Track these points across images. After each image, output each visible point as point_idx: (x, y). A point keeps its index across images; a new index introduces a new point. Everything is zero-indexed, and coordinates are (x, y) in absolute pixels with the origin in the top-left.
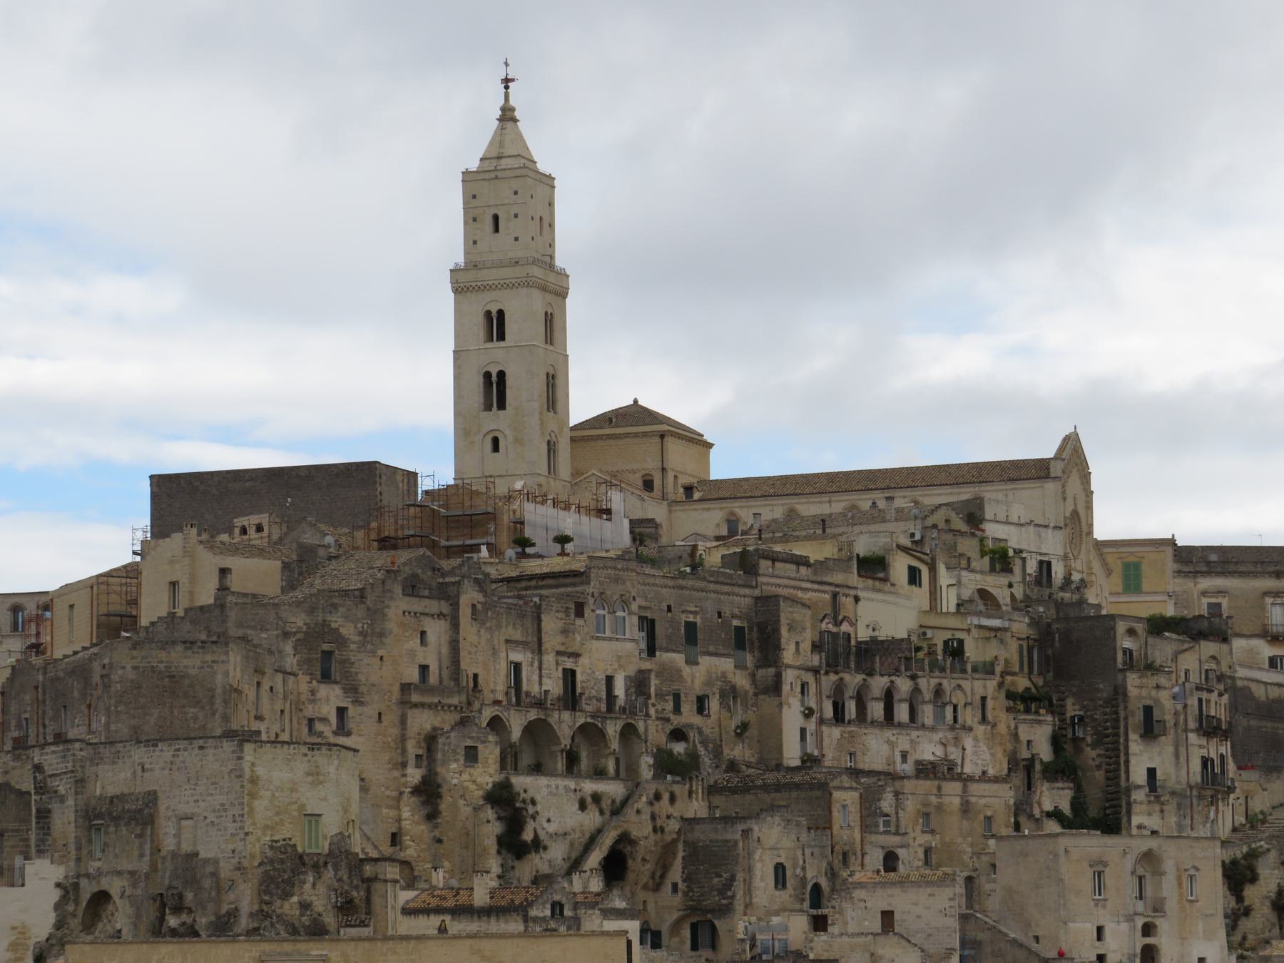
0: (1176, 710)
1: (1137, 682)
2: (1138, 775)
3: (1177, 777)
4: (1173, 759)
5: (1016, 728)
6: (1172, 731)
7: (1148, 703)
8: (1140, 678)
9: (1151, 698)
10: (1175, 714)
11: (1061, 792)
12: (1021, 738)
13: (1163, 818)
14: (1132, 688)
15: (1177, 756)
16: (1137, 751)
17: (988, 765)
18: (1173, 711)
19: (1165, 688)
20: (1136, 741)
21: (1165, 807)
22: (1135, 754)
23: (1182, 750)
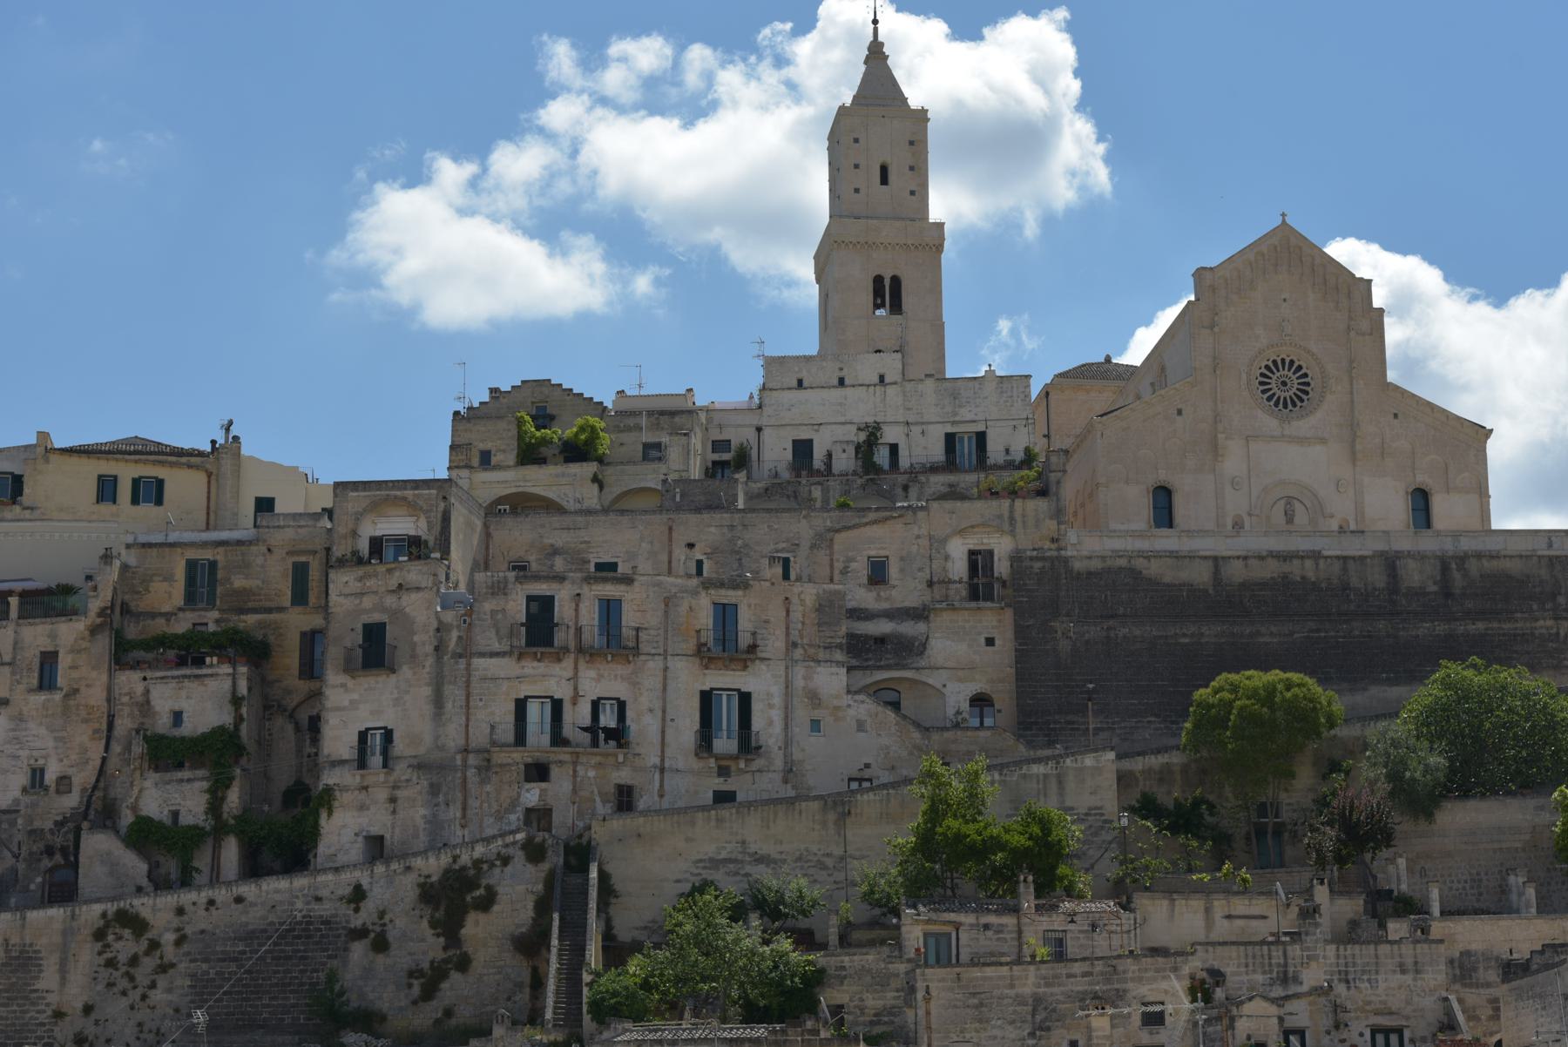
0: (440, 622)
1: (355, 586)
2: (338, 739)
3: (437, 738)
4: (428, 709)
5: (147, 692)
6: (430, 661)
7: (377, 617)
8: (360, 579)
9: (384, 610)
10: (438, 630)
11: (187, 787)
12: (157, 708)
13: (394, 812)
14: (341, 600)
15: (438, 701)
16: (346, 703)
17: (45, 757)
18: (435, 625)
19: (418, 589)
20: (343, 685)
21: (399, 793)
22: (338, 709)
23: (454, 694)
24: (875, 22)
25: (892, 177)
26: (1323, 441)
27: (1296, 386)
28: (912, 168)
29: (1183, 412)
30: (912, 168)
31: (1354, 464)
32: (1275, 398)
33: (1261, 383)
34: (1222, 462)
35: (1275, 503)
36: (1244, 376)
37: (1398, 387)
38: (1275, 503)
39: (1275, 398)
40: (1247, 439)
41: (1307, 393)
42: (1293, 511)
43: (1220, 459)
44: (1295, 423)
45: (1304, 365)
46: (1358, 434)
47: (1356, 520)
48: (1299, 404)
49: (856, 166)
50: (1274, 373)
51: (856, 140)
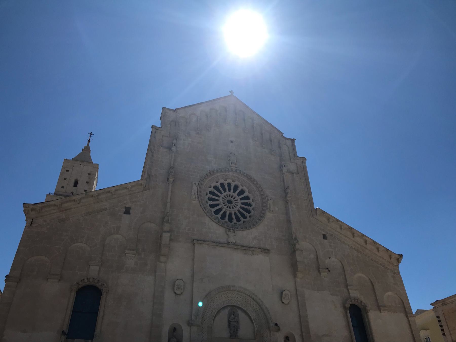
24: (89, 141)
25: (79, 185)
26: (266, 251)
27: (239, 205)
28: (87, 182)
29: (132, 211)
30: (87, 182)
31: (295, 276)
32: (222, 212)
33: (210, 199)
34: (165, 263)
35: (218, 312)
36: (195, 188)
37: (324, 213)
38: (218, 312)
39: (222, 212)
40: (193, 242)
41: (250, 205)
42: (238, 322)
43: (163, 259)
44: (240, 233)
45: (246, 190)
46: (297, 246)
47: (302, 335)
48: (242, 219)
49: (65, 179)
50: (221, 193)
51: (68, 171)
